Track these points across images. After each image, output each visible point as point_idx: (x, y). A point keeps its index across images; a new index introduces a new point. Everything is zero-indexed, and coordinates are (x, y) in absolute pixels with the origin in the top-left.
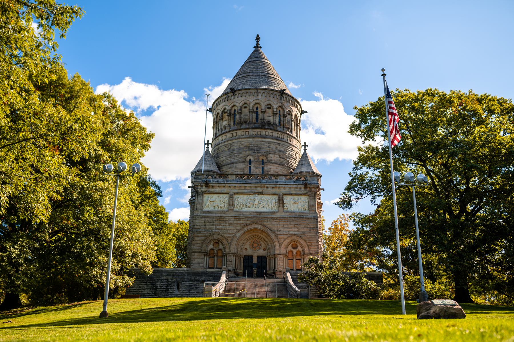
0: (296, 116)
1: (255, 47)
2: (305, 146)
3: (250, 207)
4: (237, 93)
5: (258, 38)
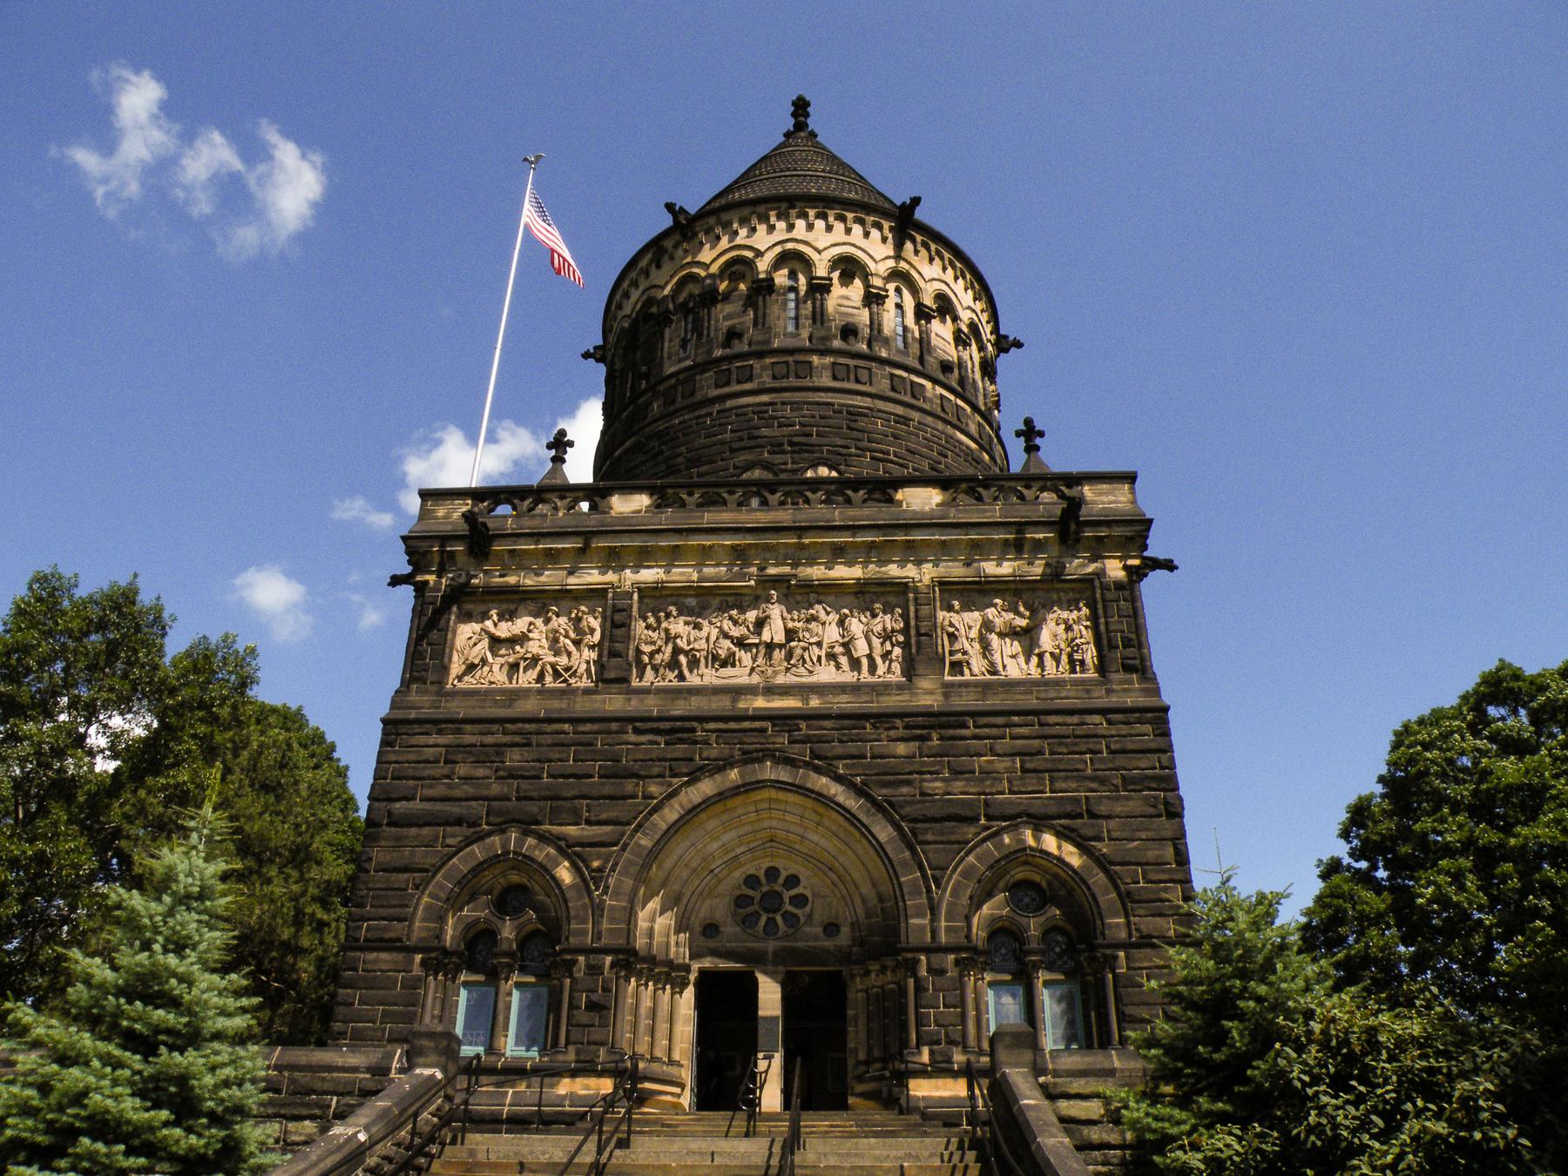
0: (973, 327)
1: (788, 135)
2: (1030, 433)
3: (729, 661)
4: (698, 226)
5: (801, 107)
